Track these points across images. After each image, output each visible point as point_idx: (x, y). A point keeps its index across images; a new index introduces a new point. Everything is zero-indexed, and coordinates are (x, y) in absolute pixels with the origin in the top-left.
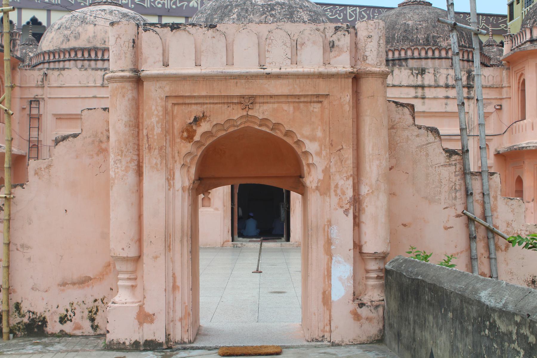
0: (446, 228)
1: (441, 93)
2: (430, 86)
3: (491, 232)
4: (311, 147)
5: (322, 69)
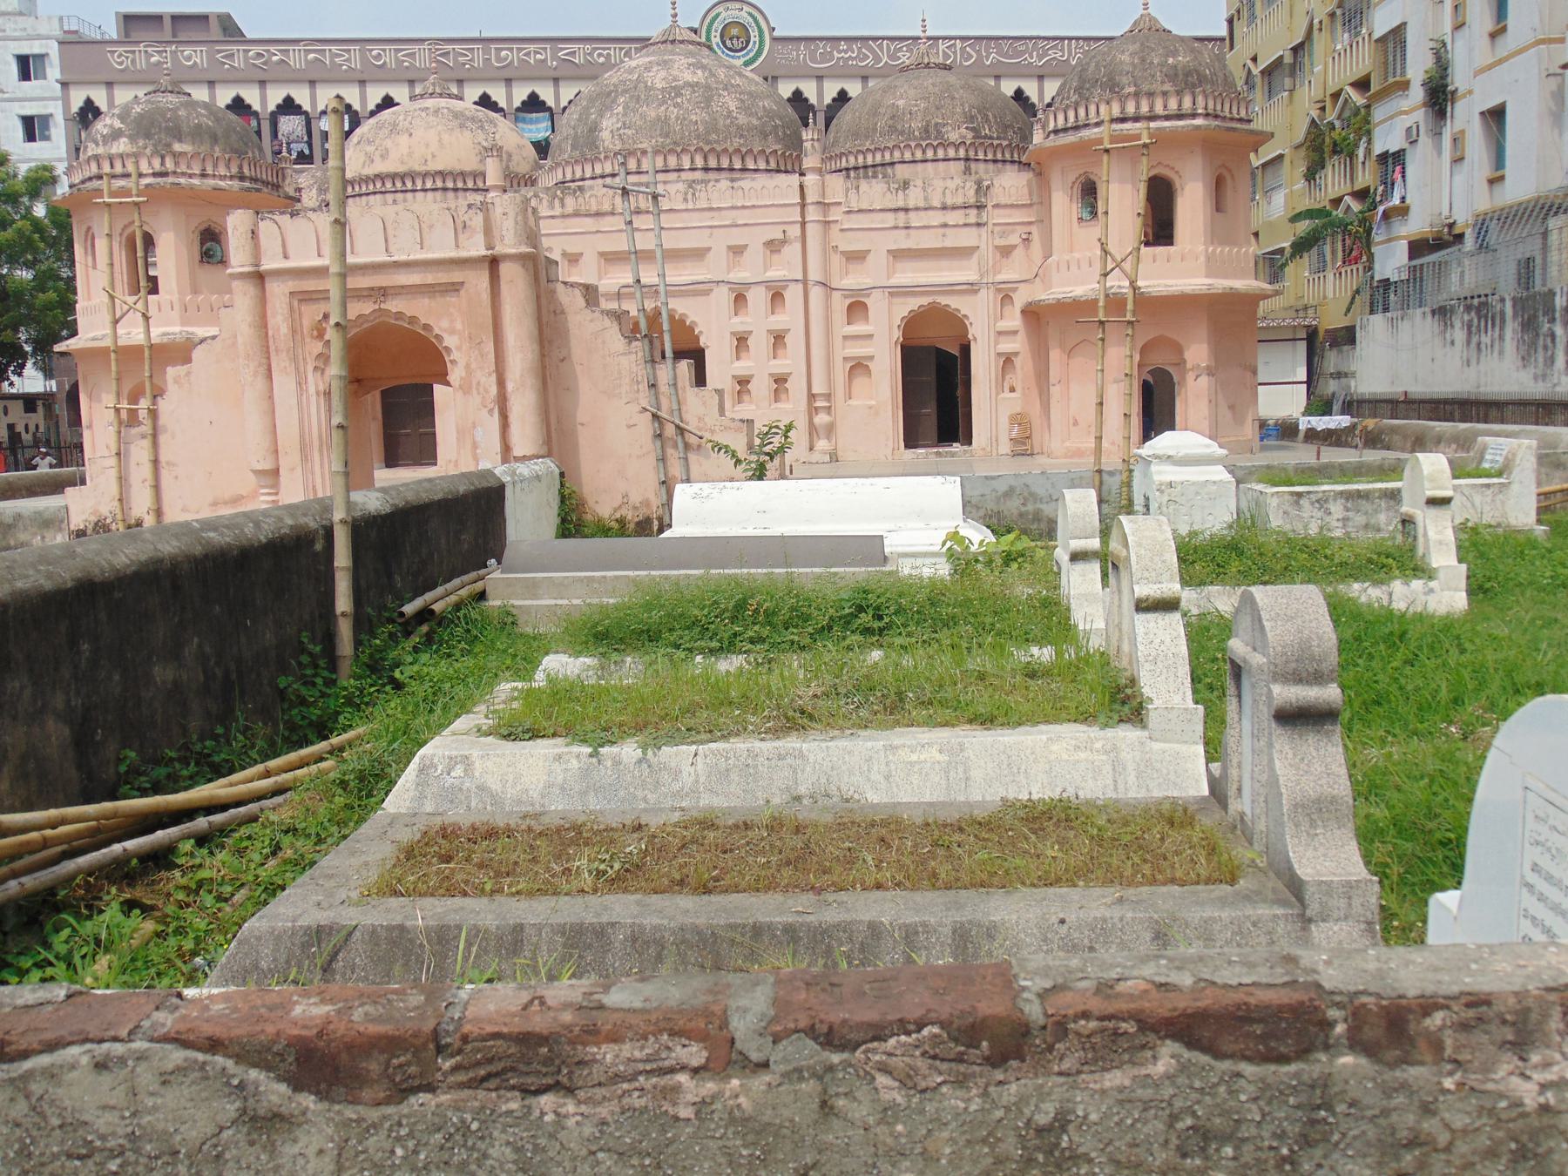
0: (629, 427)
1: (936, 218)
2: (917, 209)
3: (681, 431)
4: (450, 341)
5: (453, 254)
